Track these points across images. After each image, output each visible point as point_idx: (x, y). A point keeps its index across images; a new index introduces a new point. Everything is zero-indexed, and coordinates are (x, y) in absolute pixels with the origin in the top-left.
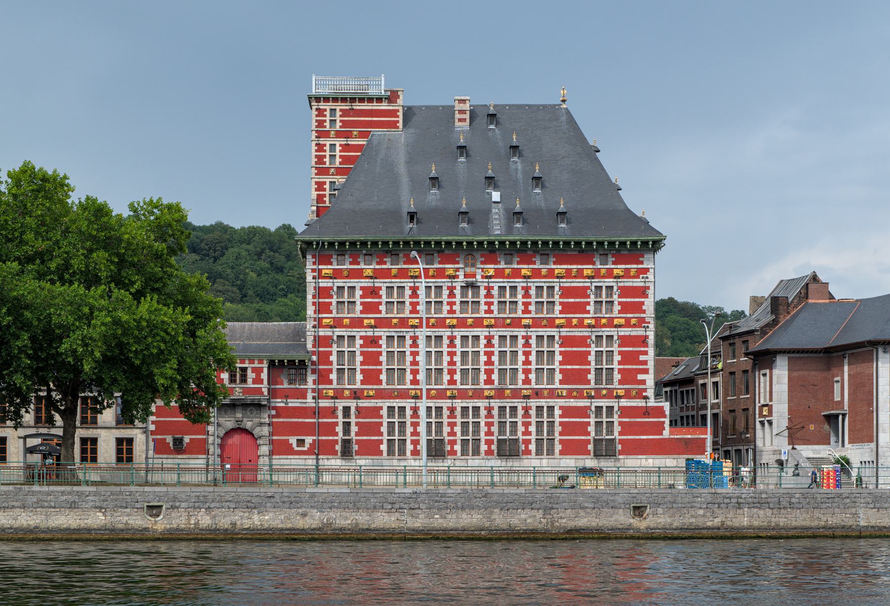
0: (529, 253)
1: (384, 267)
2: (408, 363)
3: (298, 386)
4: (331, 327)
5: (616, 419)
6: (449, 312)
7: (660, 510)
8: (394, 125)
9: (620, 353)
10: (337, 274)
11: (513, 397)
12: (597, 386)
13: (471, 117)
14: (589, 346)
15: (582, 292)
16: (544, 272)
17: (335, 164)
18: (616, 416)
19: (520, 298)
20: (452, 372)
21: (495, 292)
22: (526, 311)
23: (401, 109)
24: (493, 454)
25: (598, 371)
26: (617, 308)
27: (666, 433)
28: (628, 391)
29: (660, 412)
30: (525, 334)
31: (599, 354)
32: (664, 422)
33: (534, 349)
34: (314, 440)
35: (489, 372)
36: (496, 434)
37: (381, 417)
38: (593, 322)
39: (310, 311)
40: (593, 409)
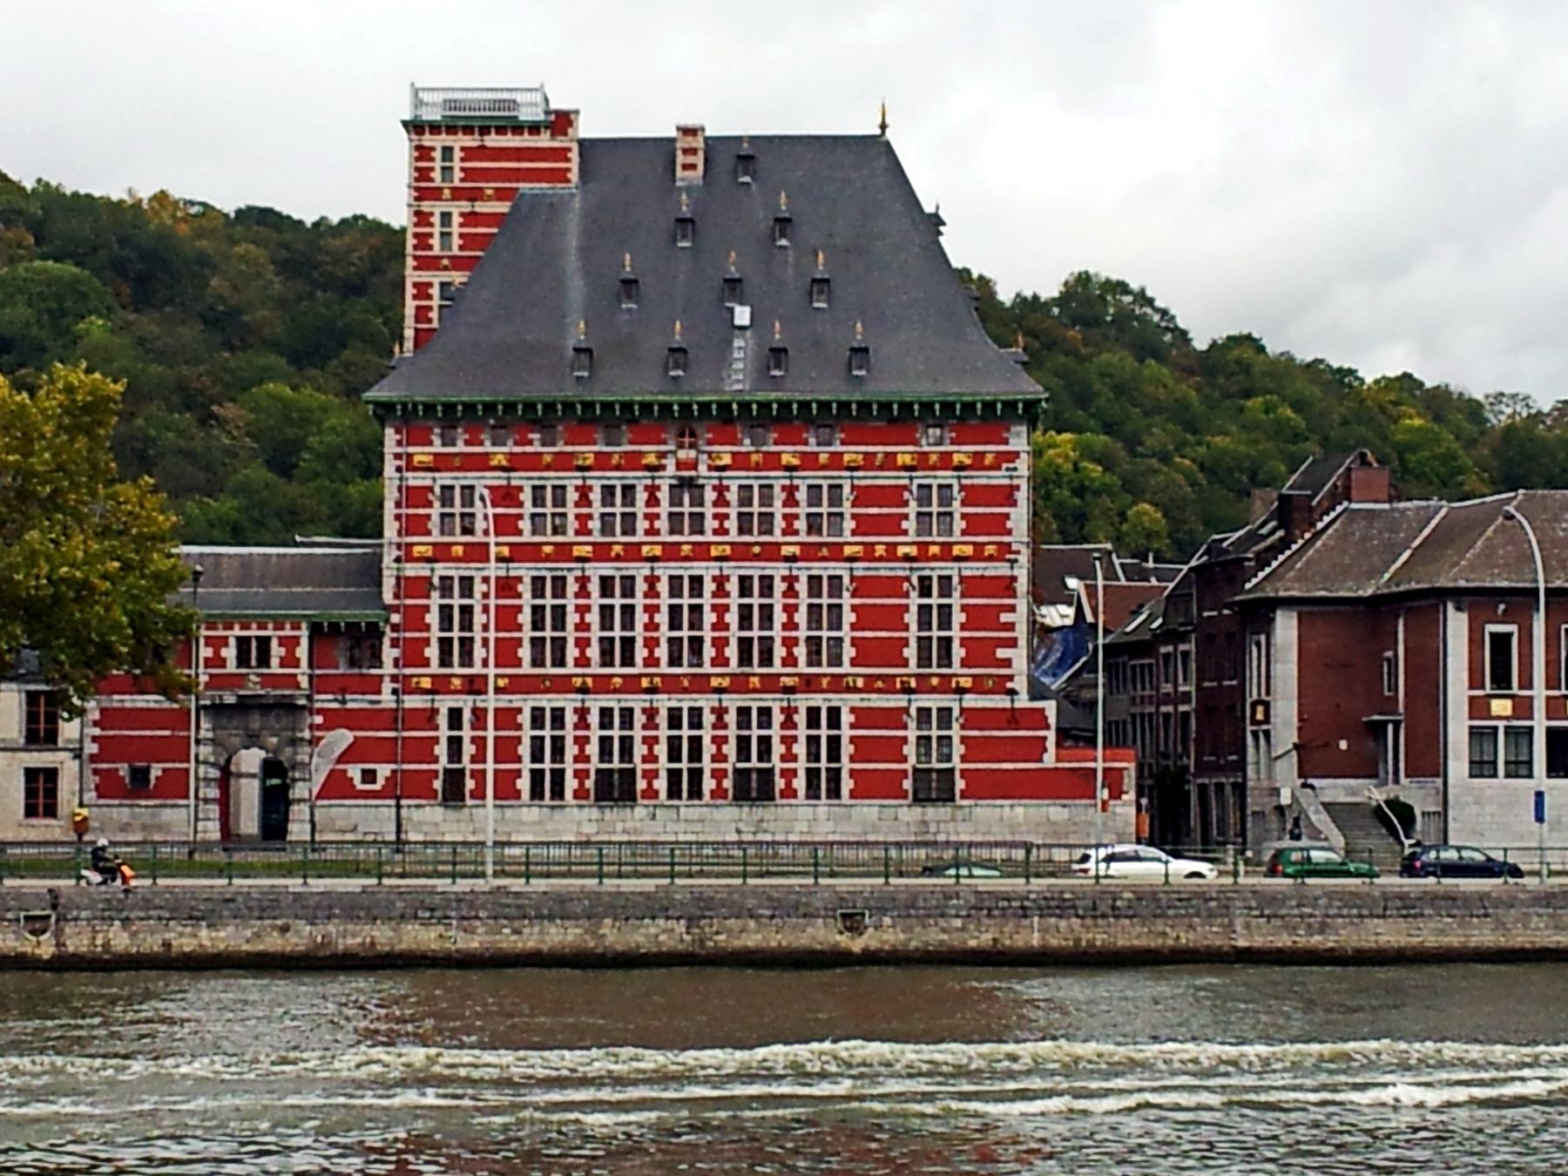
0: (797, 423)
1: (528, 449)
2: (570, 626)
3: (365, 671)
4: (428, 560)
5: (956, 732)
6: (647, 533)
7: (887, 921)
8: (561, 176)
9: (964, 608)
10: (441, 463)
12: (921, 671)
13: (706, 160)
14: (907, 595)
15: (895, 495)
16: (823, 458)
17: (450, 249)
18: (956, 726)
19: (778, 509)
20: (651, 644)
21: (732, 496)
22: (789, 530)
23: (575, 147)
24: (725, 797)
25: (924, 644)
26: (959, 525)
27: (1049, 760)
29: (1039, 718)
30: (786, 573)
31: (924, 610)
32: (1045, 738)
33: (804, 600)
34: (394, 772)
35: (720, 644)
36: (732, 757)
37: (519, 727)
38: (913, 551)
39: (390, 529)
40: (913, 712)
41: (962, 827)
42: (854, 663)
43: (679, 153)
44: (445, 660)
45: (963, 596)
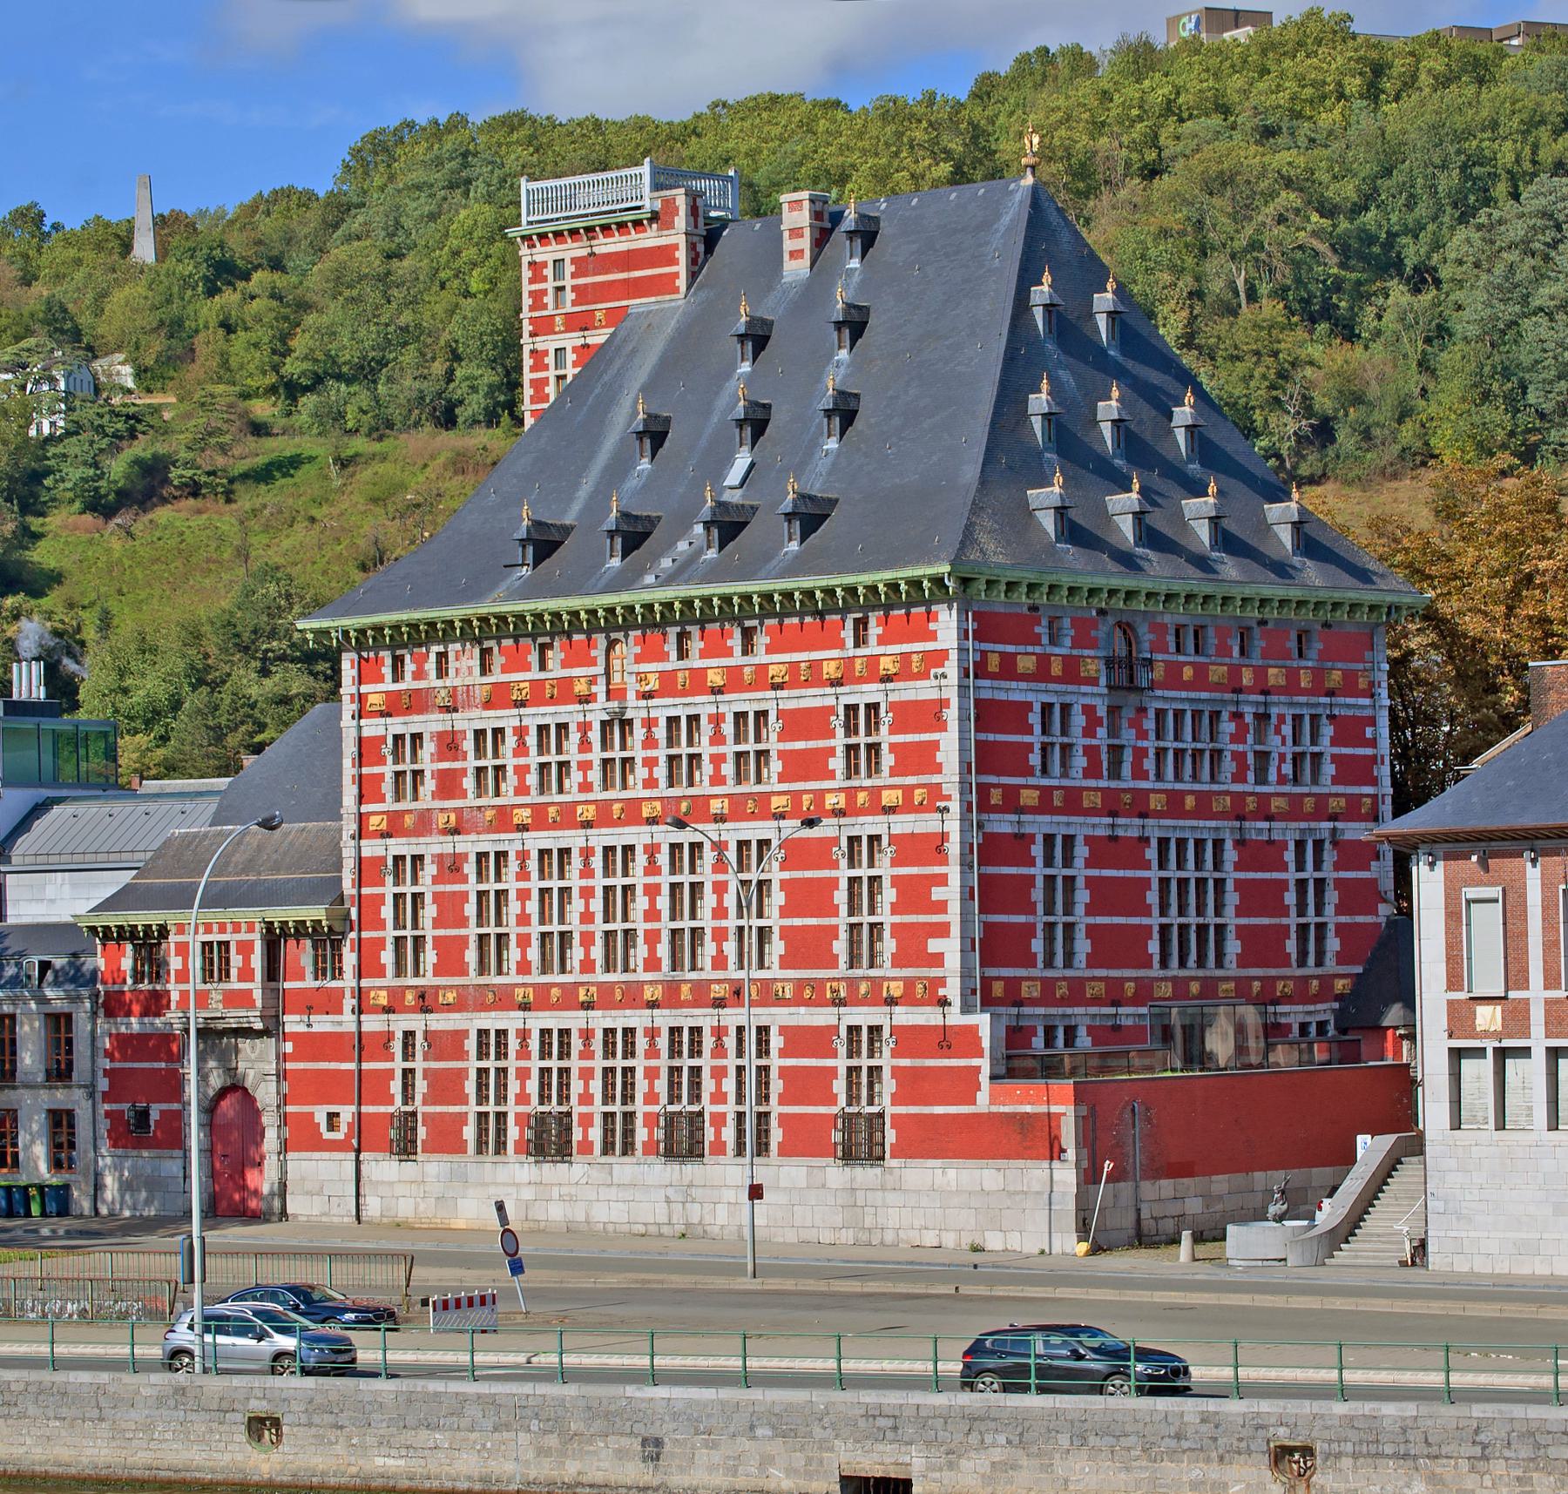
5: (885, 1061)
11: (696, 1003)
21: (660, 732)
27: (983, 1101)
28: (909, 983)
32: (978, 1069)
38: (839, 800)
40: (843, 1032)
41: (891, 1198)
42: (785, 963)
43: (786, 234)
44: (400, 971)
45: (895, 863)
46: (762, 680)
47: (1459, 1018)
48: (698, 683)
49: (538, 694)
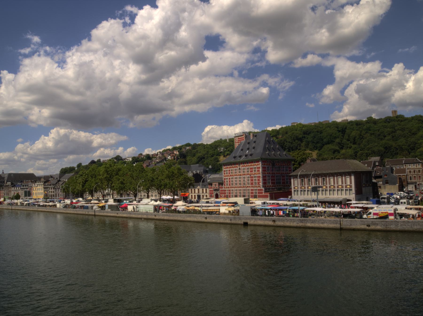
10: (226, 168)
27: (263, 194)
46: (249, 166)
47: (294, 188)
48: (244, 166)
49: (235, 167)
